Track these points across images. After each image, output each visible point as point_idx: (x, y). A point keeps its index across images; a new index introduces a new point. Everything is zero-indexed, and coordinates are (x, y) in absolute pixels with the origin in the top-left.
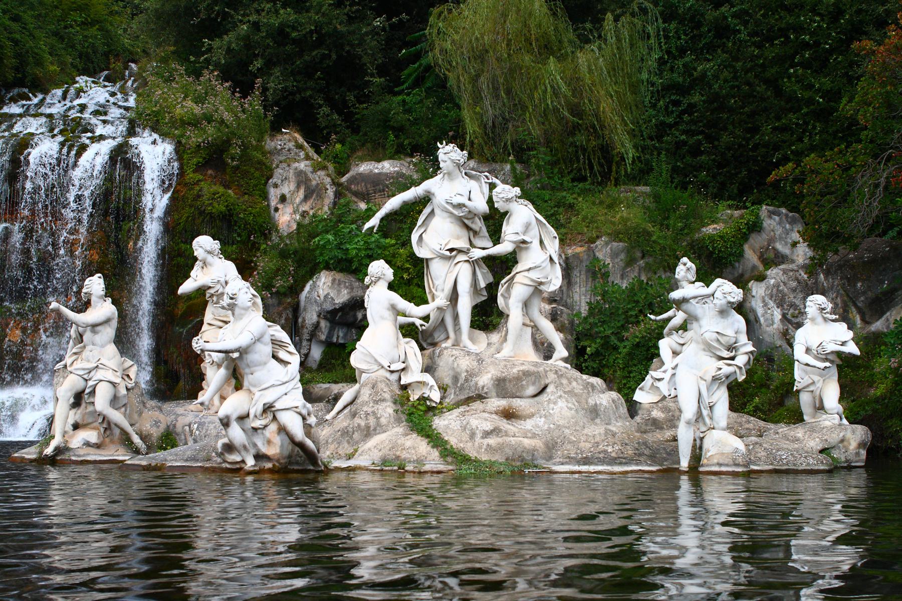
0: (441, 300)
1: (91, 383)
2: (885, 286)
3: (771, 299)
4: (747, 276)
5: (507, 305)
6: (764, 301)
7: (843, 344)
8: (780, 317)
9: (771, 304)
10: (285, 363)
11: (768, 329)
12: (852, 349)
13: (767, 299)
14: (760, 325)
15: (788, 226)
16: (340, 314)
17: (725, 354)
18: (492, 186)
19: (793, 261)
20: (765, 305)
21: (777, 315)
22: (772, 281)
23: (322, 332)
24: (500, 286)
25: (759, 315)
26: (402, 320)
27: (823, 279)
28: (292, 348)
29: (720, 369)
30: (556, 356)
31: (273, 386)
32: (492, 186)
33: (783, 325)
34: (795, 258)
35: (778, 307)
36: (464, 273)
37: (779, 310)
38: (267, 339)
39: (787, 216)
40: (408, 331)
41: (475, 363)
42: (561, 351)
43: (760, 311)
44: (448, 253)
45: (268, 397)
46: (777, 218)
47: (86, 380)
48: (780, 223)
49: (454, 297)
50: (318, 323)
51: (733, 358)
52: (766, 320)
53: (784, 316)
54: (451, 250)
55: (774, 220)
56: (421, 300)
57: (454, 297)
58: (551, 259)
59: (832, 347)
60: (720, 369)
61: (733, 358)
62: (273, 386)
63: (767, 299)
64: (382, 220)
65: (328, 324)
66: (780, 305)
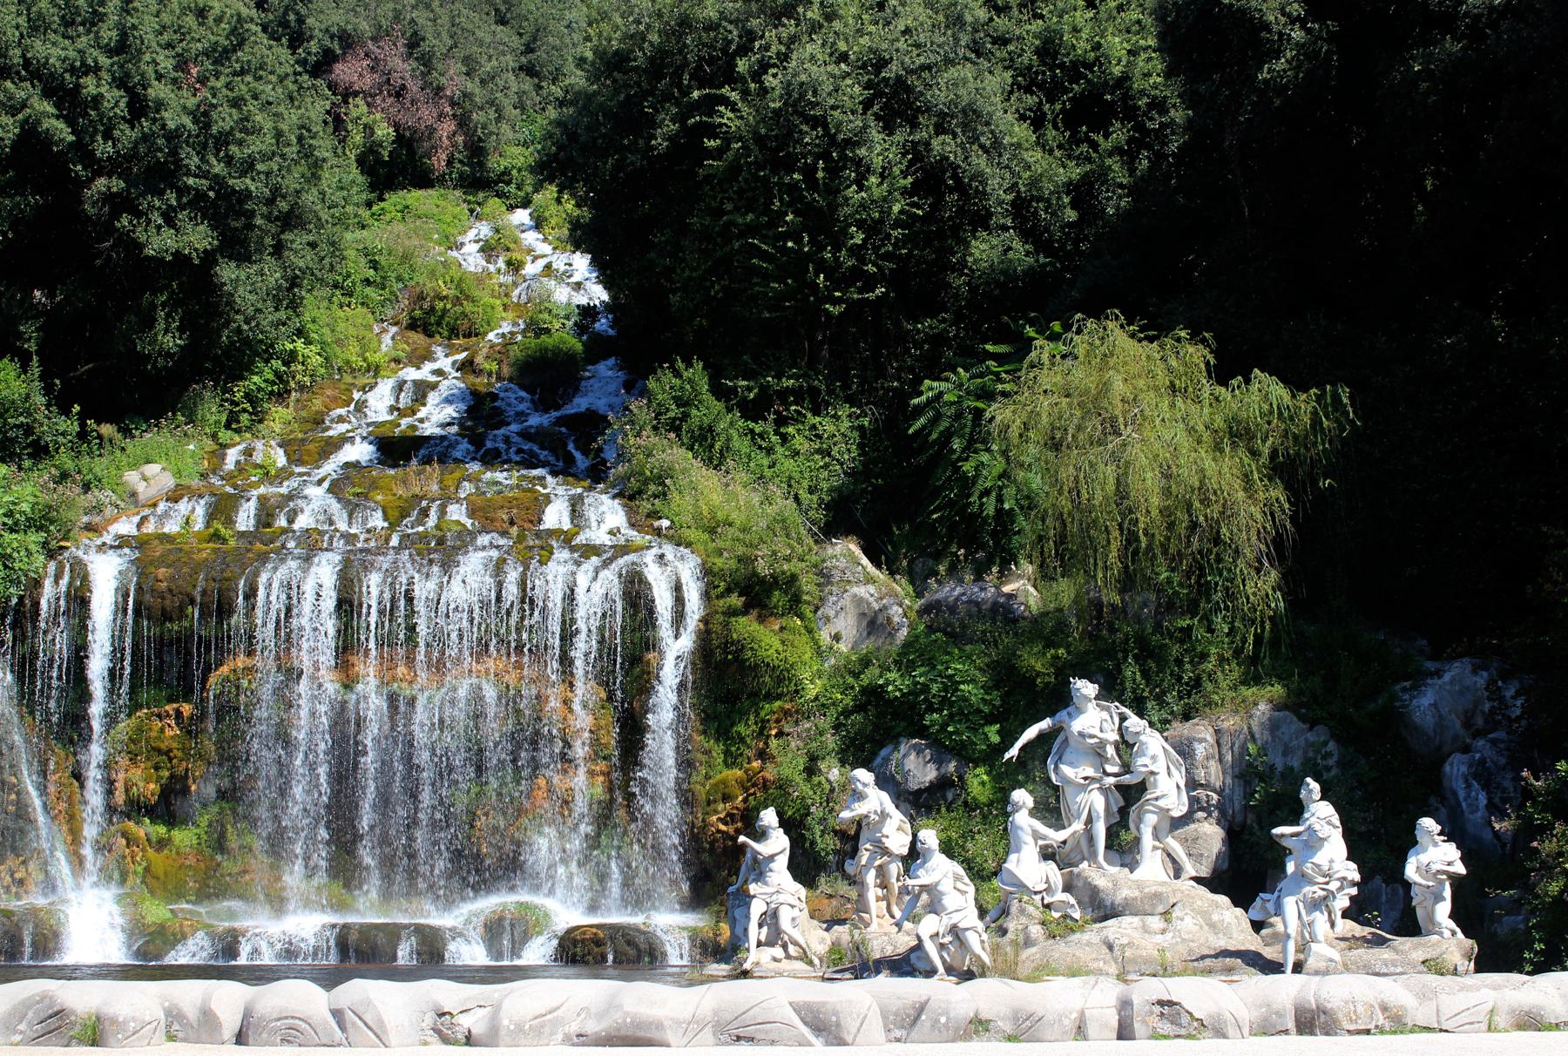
0: (1078, 826)
1: (773, 906)
5: (1138, 829)
6: (1466, 781)
7: (1449, 864)
8: (1485, 802)
10: (963, 893)
14: (1462, 811)
16: (925, 795)
17: (1321, 880)
18: (1123, 718)
20: (1469, 786)
21: (1483, 800)
22: (1478, 756)
25: (1461, 799)
26: (1041, 842)
28: (967, 880)
30: (1185, 876)
32: (1123, 718)
36: (1097, 801)
38: (950, 875)
40: (1047, 854)
41: (1110, 885)
43: (1462, 794)
44: (1082, 781)
45: (955, 918)
49: (1090, 821)
52: (1469, 805)
53: (1490, 800)
54: (1085, 778)
55: (1482, 676)
56: (1059, 826)
57: (1090, 821)
58: (1178, 787)
61: (1327, 883)
64: (1021, 750)
66: (1486, 786)
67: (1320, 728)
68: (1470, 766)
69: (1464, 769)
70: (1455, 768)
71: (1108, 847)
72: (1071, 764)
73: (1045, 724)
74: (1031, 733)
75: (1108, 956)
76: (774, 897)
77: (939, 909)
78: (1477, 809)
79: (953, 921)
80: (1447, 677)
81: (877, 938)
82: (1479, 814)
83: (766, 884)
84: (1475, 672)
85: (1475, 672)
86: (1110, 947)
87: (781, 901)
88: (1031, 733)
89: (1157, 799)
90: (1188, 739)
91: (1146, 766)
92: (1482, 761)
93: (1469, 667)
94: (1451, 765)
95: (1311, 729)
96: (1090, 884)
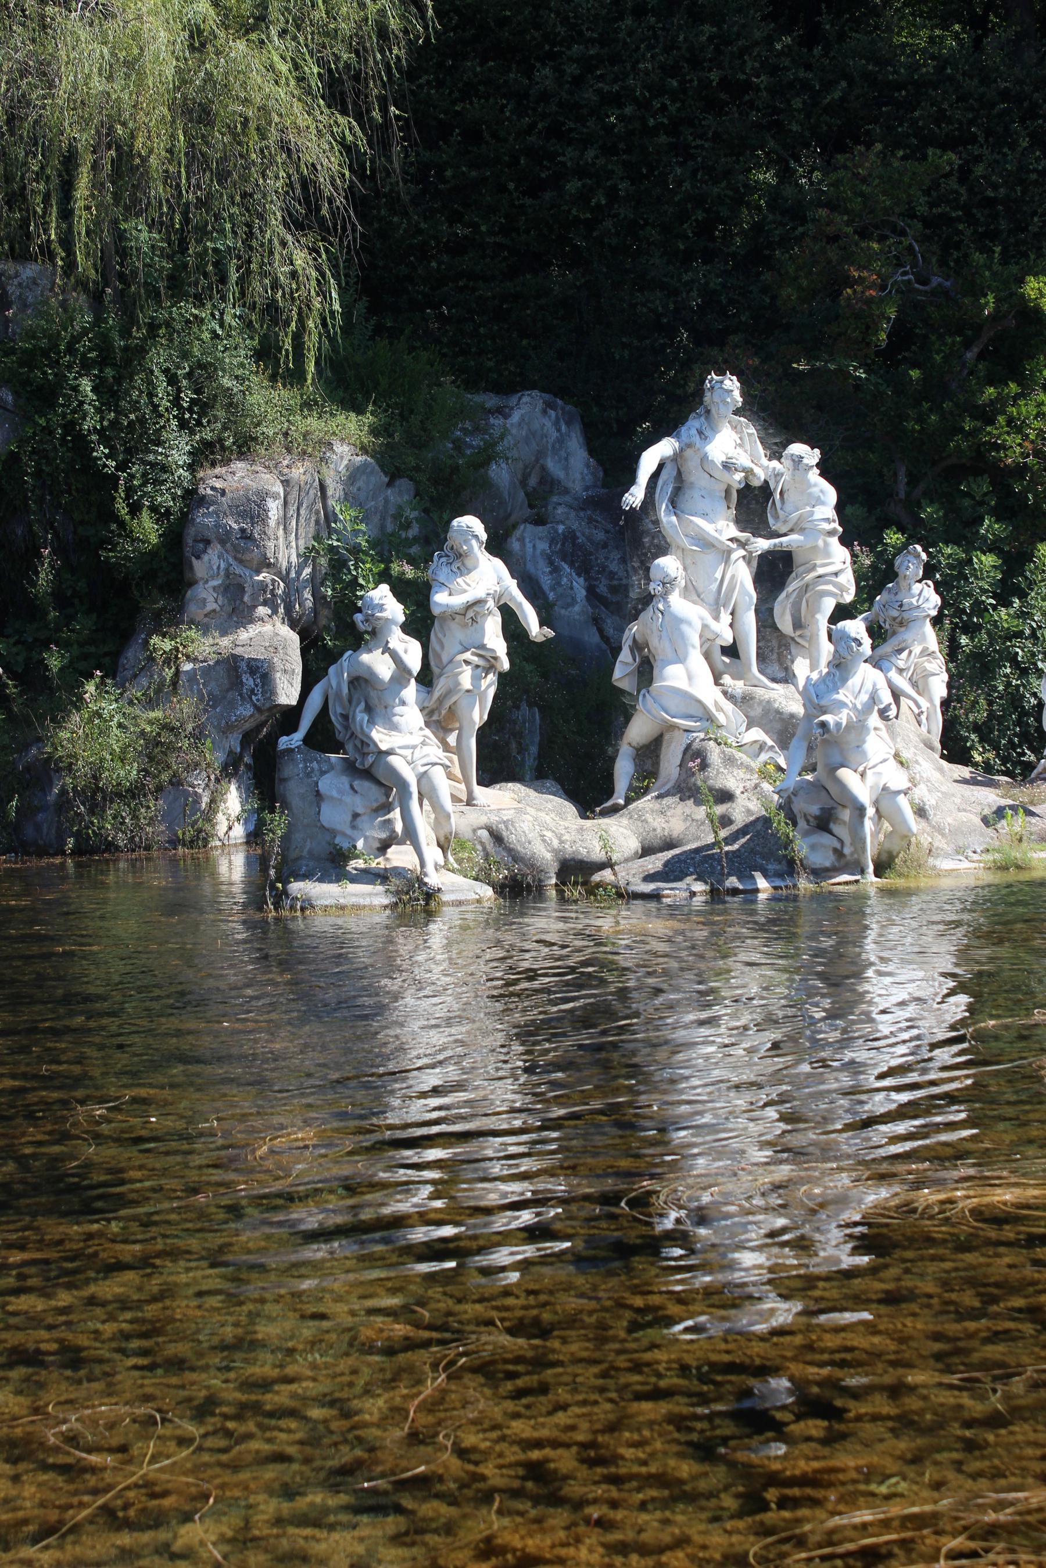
3: (564, 560)
4: (514, 518)
6: (551, 563)
8: (584, 593)
9: (566, 566)
11: (563, 611)
13: (557, 561)
15: (564, 428)
19: (566, 491)
20: (556, 570)
22: (561, 528)
25: (546, 587)
33: (593, 607)
34: (570, 485)
35: (579, 575)
37: (581, 580)
39: (563, 409)
44: (729, 543)
46: (553, 413)
48: (556, 423)
53: (591, 591)
63: (557, 561)
67: (404, 483)
68: (552, 542)
69: (543, 546)
70: (529, 546)
71: (761, 657)
72: (704, 515)
73: (664, 448)
76: (418, 753)
78: (574, 601)
80: (516, 417)
82: (577, 608)
83: (394, 727)
84: (544, 412)
89: (836, 574)
90: (258, 493)
92: (570, 536)
93: (540, 404)
94: (522, 540)
95: (389, 484)
96: (778, 712)
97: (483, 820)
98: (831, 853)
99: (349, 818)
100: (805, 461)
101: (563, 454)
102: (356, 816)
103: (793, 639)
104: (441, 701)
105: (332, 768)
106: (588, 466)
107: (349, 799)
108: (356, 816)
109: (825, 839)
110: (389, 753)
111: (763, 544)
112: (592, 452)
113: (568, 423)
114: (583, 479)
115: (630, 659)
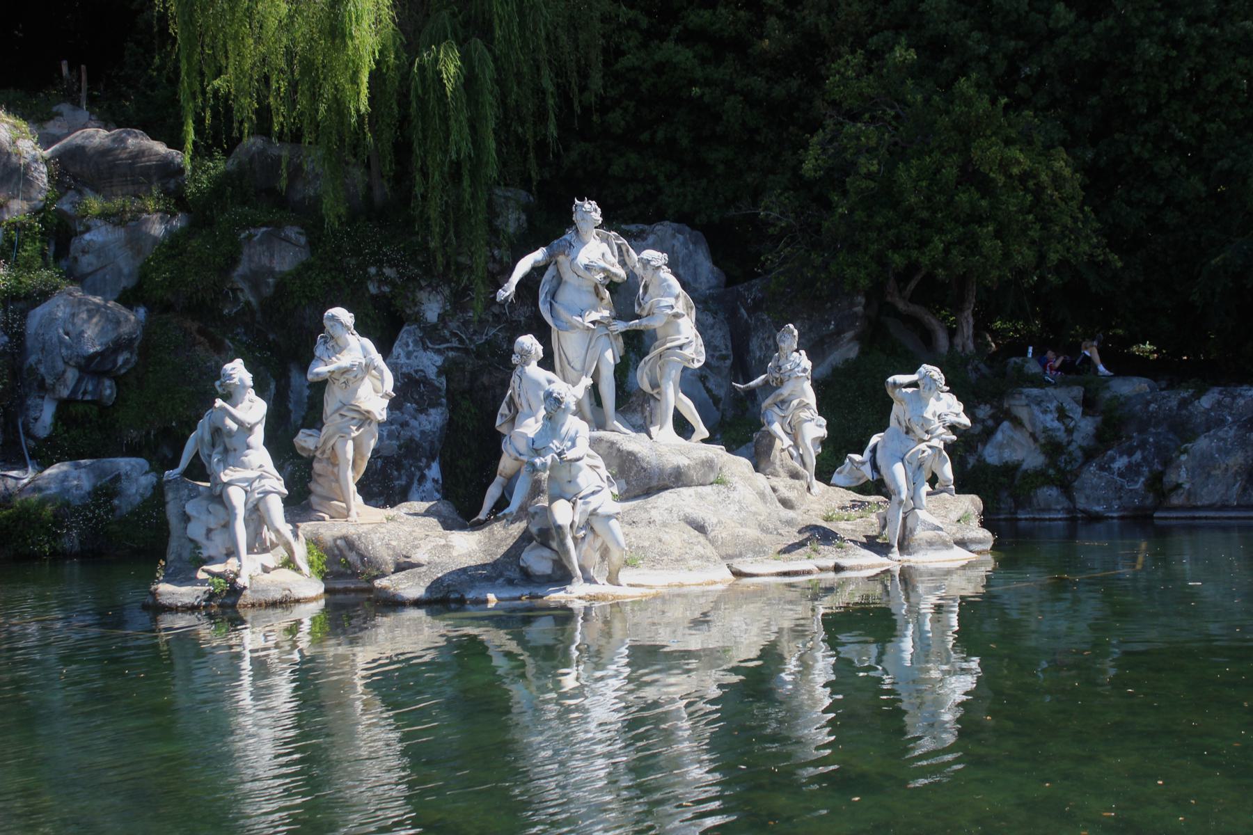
0: (587, 381)
2: (832, 327)
5: (655, 385)
7: (957, 415)
12: (965, 421)
15: (691, 247)
16: (99, 359)
23: (66, 386)
24: (643, 362)
27: (746, 316)
29: (924, 452)
31: (593, 493)
34: (697, 286)
42: (702, 431)
44: (591, 326)
46: (680, 237)
47: (246, 492)
48: (685, 244)
49: (596, 376)
50: (64, 372)
51: (928, 441)
59: (952, 419)
60: (924, 452)
62: (593, 493)
65: (77, 374)
73: (539, 255)
74: (524, 266)
75: (701, 538)
77: (570, 489)
79: (591, 508)
81: (374, 531)
85: (674, 236)
86: (701, 528)
87: (268, 488)
88: (524, 266)
89: (681, 347)
91: (672, 307)
93: (670, 231)
97: (344, 532)
98: (550, 564)
99: (204, 531)
100: (652, 263)
101: (691, 264)
102: (209, 531)
103: (652, 395)
104: (325, 443)
105: (198, 494)
106: (712, 272)
107: (204, 517)
108: (209, 531)
109: (546, 553)
110: (229, 484)
111: (621, 326)
112: (715, 263)
113: (695, 243)
114: (708, 282)
115: (507, 412)
